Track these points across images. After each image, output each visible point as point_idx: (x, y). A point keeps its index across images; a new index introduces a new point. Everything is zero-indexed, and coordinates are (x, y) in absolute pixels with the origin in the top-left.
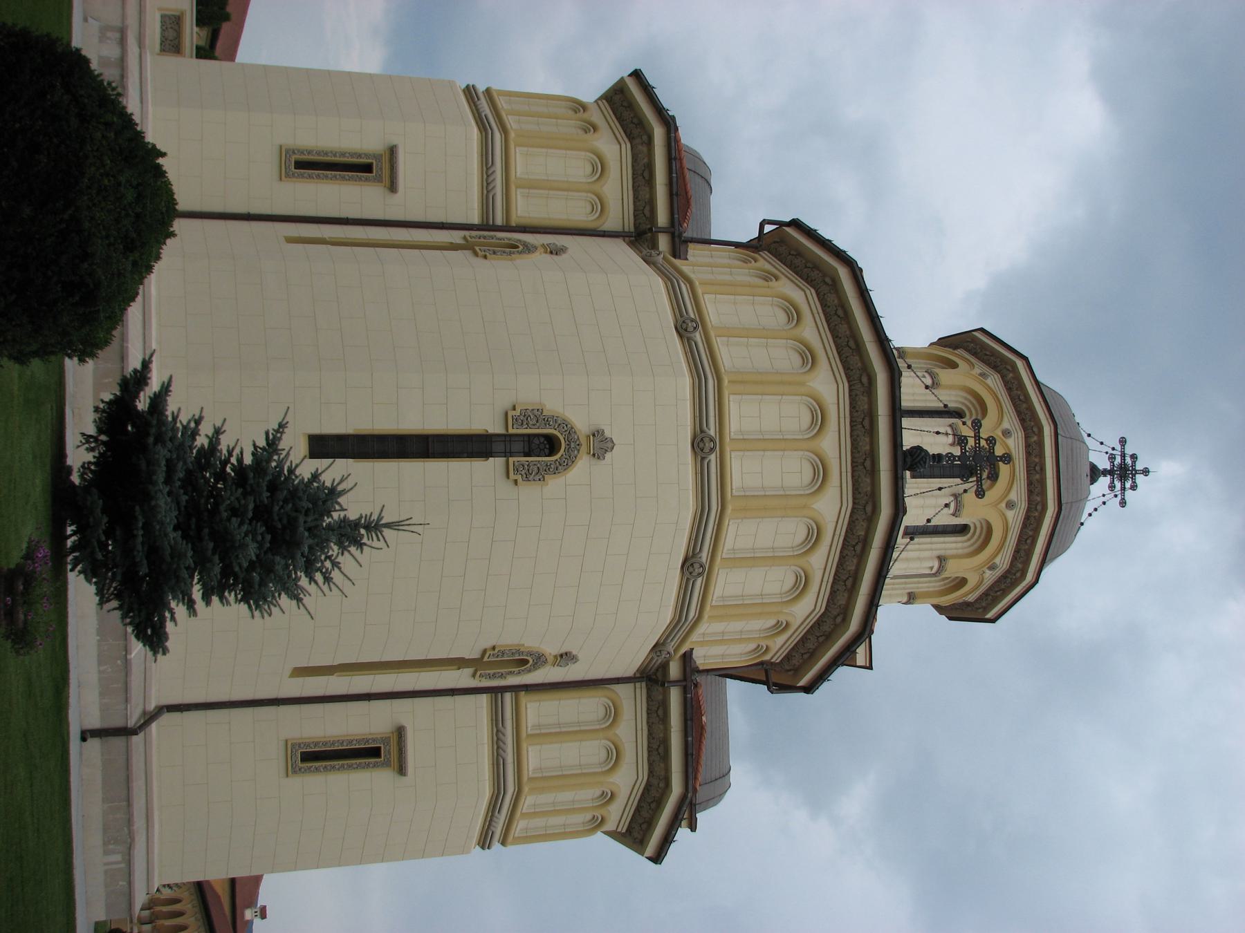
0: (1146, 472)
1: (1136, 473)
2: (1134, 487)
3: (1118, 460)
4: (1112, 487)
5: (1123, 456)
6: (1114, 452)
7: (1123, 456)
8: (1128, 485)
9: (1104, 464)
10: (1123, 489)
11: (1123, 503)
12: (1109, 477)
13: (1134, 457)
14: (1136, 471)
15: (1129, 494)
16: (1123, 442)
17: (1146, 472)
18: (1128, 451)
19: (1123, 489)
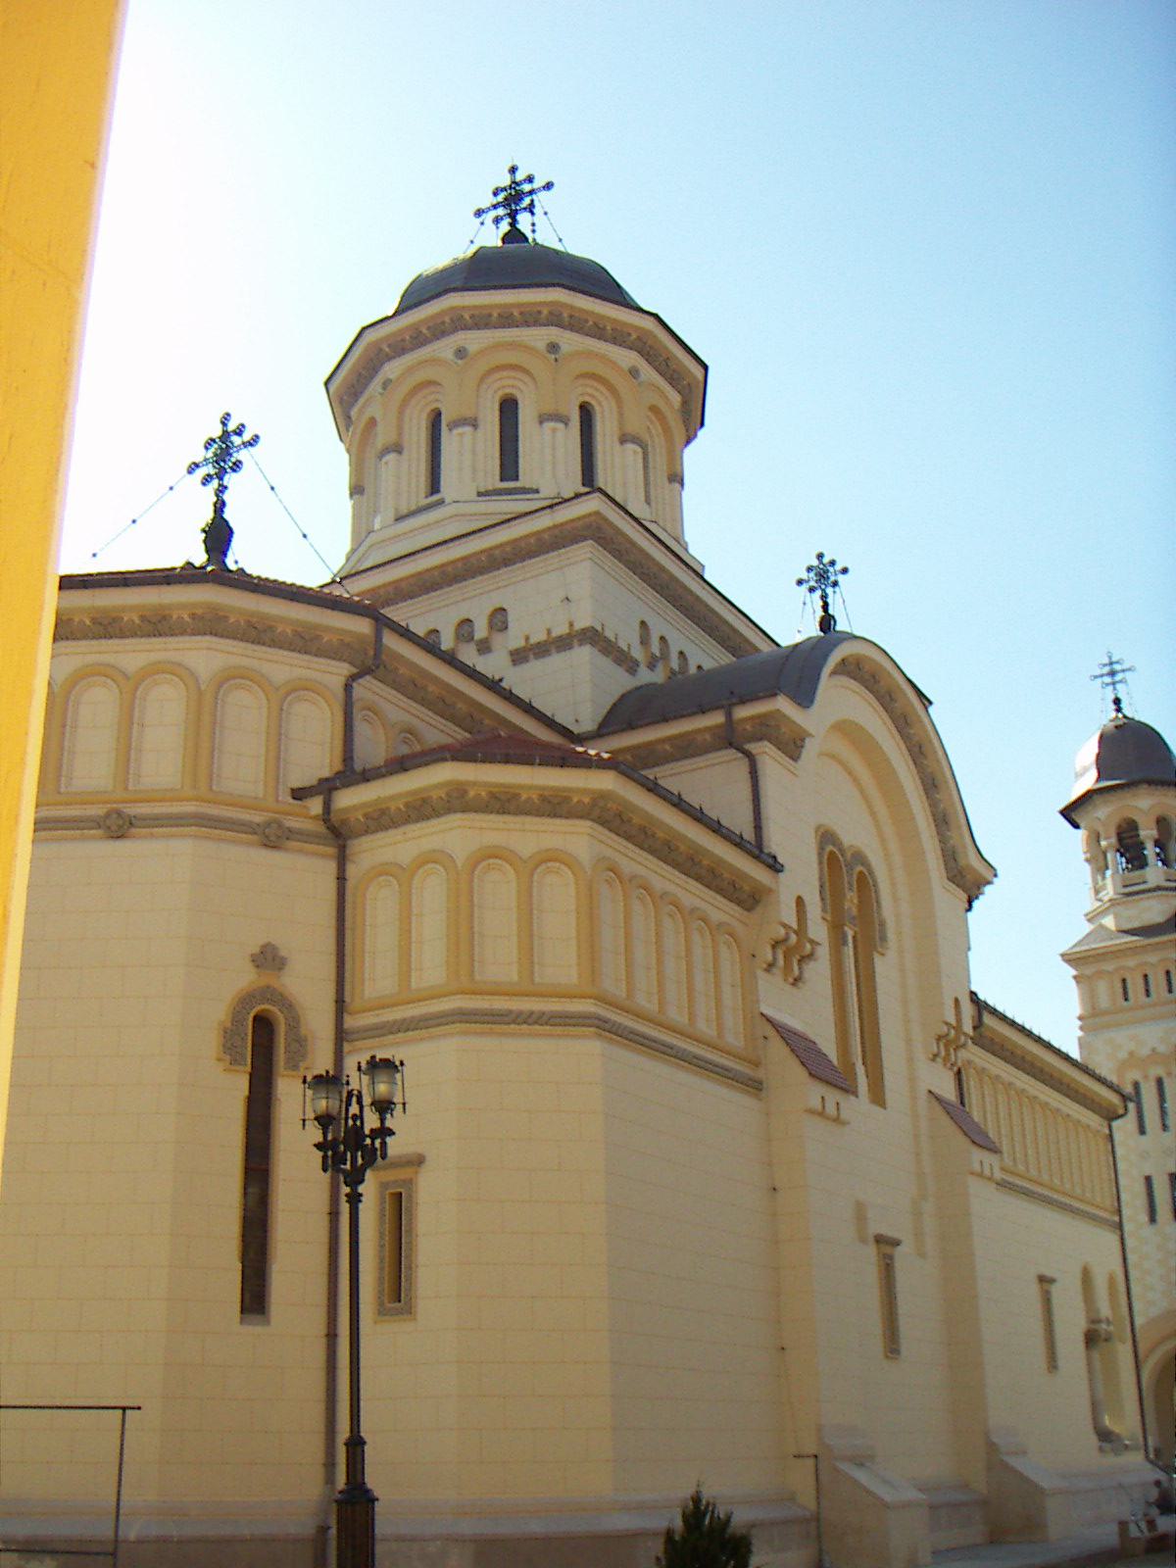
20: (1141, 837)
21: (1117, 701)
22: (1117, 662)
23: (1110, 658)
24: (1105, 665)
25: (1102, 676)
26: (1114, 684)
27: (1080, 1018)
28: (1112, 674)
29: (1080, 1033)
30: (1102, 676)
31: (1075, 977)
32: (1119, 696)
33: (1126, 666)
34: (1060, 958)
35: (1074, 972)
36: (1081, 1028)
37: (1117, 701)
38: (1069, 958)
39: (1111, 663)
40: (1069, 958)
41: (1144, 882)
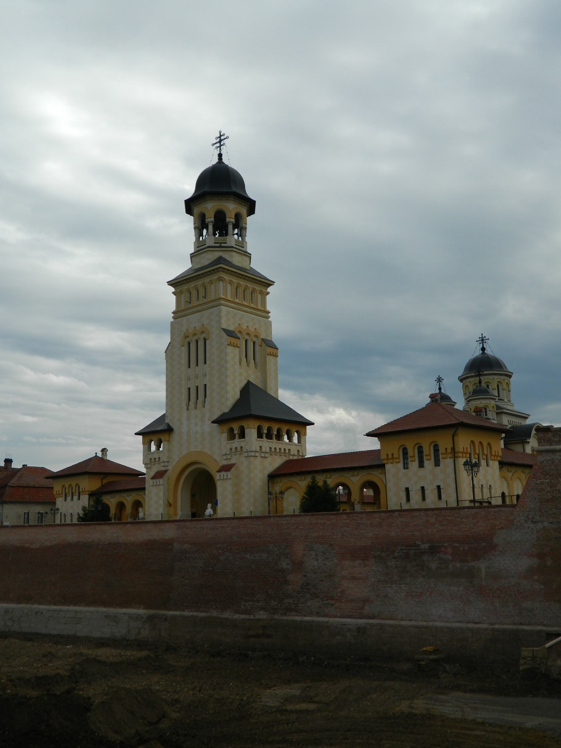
0: (482, 334)
1: (482, 337)
2: (485, 337)
3: (480, 342)
4: (486, 342)
5: (479, 341)
6: (479, 343)
7: (479, 341)
8: (485, 338)
9: (481, 345)
10: (486, 339)
11: (488, 339)
12: (484, 344)
13: (480, 338)
14: (482, 337)
15: (487, 338)
16: (477, 341)
17: (482, 334)
18: (478, 339)
19: (486, 339)
20: (206, 222)
21: (220, 155)
22: (222, 135)
23: (220, 134)
24: (218, 138)
25: (216, 143)
26: (220, 147)
27: (173, 313)
28: (220, 142)
29: (173, 320)
30: (216, 143)
31: (173, 293)
32: (221, 152)
33: (225, 137)
34: (167, 283)
35: (173, 289)
36: (173, 318)
37: (220, 155)
38: (171, 283)
39: (221, 136)
40: (171, 283)
41: (205, 245)
